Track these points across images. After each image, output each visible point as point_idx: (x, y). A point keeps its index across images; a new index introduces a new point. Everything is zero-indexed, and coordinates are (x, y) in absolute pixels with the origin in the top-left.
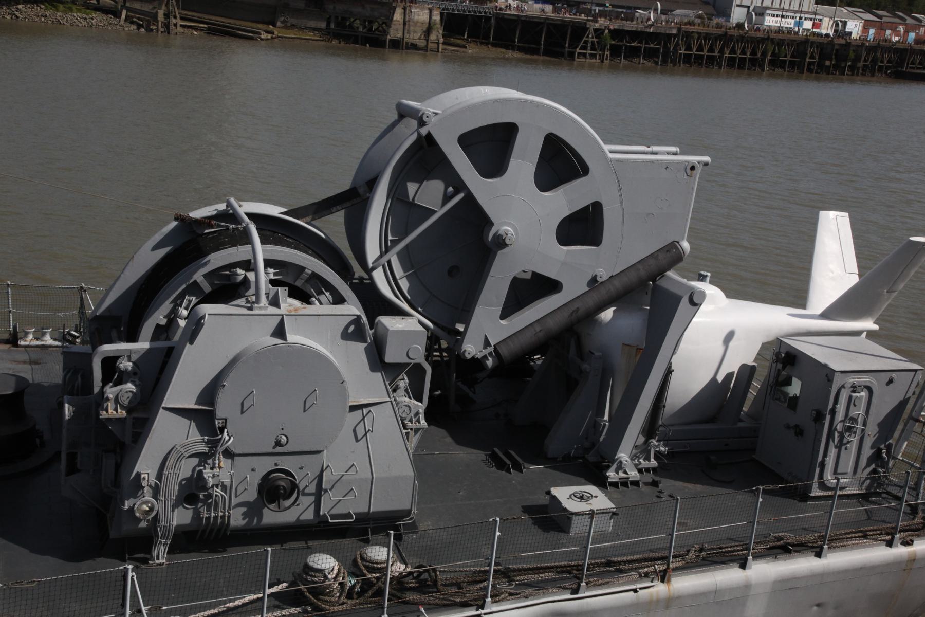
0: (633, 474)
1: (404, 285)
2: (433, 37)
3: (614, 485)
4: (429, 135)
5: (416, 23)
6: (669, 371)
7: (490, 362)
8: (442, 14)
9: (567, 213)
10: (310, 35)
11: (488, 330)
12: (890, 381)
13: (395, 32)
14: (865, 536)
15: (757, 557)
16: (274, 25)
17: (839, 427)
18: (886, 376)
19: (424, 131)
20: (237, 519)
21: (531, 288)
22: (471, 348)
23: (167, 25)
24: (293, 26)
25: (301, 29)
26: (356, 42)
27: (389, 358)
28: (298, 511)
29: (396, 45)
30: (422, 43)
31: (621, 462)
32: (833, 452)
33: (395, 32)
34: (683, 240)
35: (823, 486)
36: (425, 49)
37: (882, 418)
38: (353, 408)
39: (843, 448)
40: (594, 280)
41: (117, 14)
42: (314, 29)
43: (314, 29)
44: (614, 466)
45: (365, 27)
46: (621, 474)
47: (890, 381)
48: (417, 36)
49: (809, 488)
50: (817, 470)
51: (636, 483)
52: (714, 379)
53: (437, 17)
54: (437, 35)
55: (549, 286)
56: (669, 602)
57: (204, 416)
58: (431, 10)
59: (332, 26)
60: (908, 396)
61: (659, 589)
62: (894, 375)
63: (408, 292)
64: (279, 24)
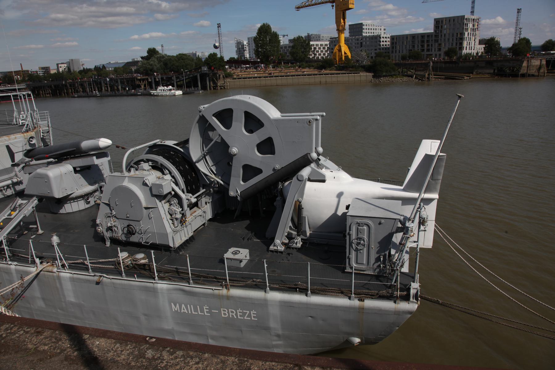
0: (281, 248)
1: (214, 169)
2: (542, 71)
3: (272, 251)
4: (203, 115)
5: (533, 66)
6: (299, 209)
7: (239, 198)
8: (547, 61)
9: (259, 142)
10: (487, 76)
11: (238, 187)
13: (523, 71)
14: (342, 293)
15: (272, 289)
16: (472, 73)
17: (355, 241)
18: (378, 220)
19: (201, 114)
20: (123, 238)
21: (250, 171)
22: (232, 193)
23: (428, 78)
24: (480, 73)
25: (483, 74)
26: (506, 76)
27: (154, 193)
28: (134, 239)
29: (523, 76)
30: (536, 74)
32: (353, 254)
33: (523, 71)
34: (312, 152)
36: (538, 76)
38: (146, 208)
40: (274, 170)
41: (412, 77)
42: (488, 73)
43: (488, 73)
44: (273, 244)
45: (510, 70)
46: (275, 248)
47: (380, 224)
48: (533, 71)
49: (345, 268)
50: (347, 260)
51: (281, 252)
52: (335, 215)
53: (544, 62)
54: (544, 70)
55: (259, 171)
56: (228, 298)
57: (108, 205)
58: (541, 60)
59: (496, 71)
61: (224, 291)
62: (383, 221)
63: (216, 171)
64: (474, 73)
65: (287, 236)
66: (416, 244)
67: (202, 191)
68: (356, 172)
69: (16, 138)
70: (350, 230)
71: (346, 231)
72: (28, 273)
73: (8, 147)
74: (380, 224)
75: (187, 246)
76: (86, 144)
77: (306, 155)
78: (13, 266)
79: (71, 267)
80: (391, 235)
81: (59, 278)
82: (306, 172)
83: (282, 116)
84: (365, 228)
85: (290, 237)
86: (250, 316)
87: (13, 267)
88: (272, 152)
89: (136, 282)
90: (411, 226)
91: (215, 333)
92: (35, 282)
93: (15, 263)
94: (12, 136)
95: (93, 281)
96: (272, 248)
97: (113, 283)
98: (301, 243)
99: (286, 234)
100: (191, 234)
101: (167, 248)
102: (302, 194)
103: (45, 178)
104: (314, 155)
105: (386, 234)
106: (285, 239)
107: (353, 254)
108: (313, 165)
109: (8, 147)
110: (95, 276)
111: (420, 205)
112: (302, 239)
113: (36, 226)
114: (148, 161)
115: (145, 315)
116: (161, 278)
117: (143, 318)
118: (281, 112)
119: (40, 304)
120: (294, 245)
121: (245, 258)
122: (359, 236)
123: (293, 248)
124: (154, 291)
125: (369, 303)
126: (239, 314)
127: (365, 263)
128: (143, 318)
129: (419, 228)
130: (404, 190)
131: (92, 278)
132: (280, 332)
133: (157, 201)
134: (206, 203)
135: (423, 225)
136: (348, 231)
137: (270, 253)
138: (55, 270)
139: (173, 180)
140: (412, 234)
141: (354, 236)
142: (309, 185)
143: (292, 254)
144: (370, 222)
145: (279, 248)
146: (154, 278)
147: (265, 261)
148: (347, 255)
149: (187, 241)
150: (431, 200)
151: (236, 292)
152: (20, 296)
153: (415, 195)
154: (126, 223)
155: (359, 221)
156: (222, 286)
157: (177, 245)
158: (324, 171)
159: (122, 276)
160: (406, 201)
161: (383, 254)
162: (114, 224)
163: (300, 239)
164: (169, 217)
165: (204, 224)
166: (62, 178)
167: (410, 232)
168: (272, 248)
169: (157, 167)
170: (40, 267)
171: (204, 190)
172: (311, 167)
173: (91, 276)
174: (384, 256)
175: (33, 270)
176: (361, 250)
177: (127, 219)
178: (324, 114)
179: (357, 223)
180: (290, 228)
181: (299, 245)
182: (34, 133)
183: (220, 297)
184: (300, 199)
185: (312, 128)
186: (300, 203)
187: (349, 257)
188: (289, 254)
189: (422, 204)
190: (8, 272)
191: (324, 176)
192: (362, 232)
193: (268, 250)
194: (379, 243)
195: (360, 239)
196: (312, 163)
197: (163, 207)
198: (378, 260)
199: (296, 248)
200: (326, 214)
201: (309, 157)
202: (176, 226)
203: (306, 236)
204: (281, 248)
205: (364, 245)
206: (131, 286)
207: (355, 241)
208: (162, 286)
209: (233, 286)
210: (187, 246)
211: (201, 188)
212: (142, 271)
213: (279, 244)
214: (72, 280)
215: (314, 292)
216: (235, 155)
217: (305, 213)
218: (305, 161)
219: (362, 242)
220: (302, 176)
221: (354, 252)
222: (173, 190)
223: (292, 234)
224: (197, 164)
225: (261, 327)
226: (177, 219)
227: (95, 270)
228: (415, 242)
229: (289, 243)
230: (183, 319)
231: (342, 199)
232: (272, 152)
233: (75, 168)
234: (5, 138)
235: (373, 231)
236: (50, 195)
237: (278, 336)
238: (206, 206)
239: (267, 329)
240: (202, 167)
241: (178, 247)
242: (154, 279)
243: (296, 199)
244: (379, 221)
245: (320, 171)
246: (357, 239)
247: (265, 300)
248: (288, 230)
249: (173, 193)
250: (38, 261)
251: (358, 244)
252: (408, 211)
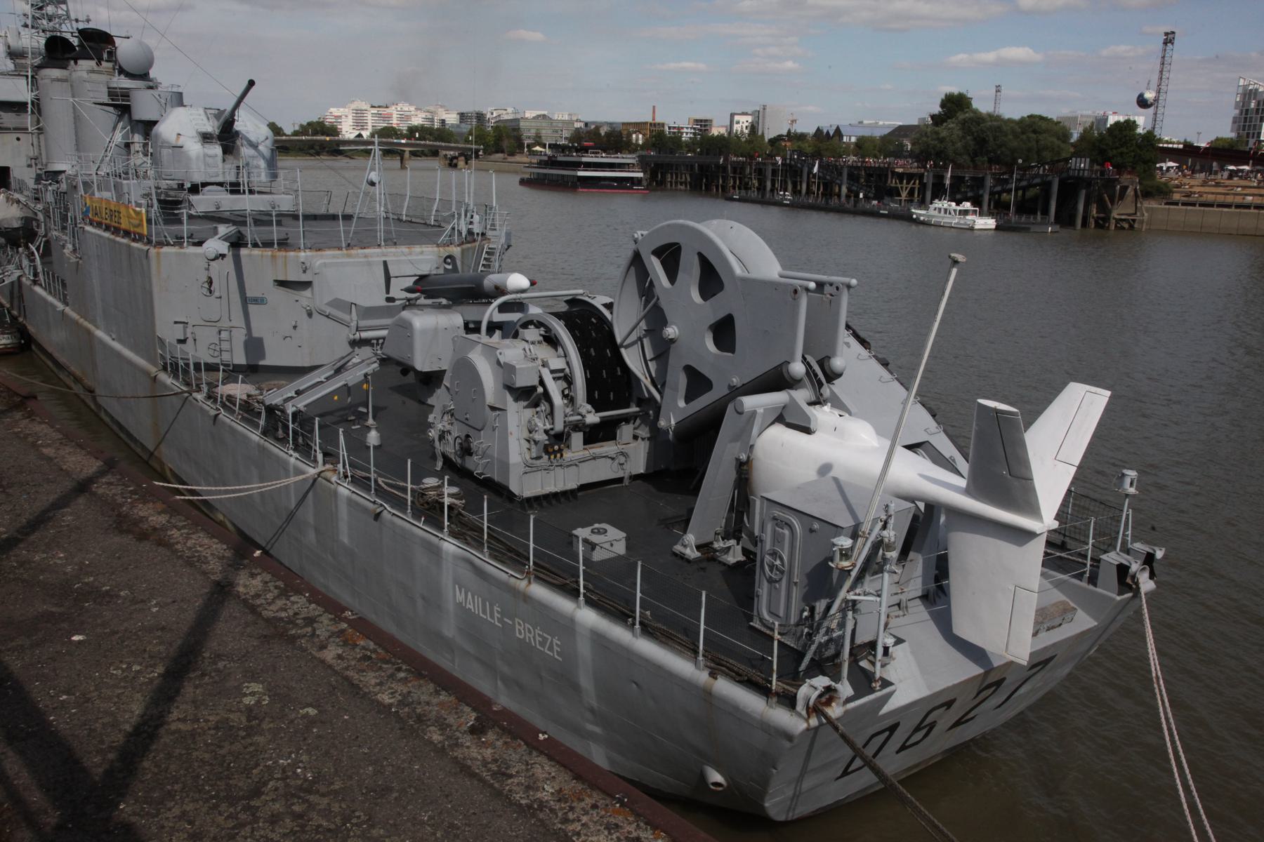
0: (692, 553)
3: (675, 554)
35: (761, 620)
38: (493, 408)
51: (688, 561)
56: (527, 598)
61: (522, 585)
67: (634, 409)
69: (422, 253)
72: (303, 473)
73: (385, 263)
75: (550, 504)
76: (491, 280)
78: (293, 458)
79: (355, 481)
81: (335, 493)
83: (781, 276)
86: (551, 648)
87: (292, 460)
88: (732, 349)
89: (420, 530)
91: (505, 669)
92: (310, 494)
93: (296, 455)
94: (417, 249)
95: (365, 510)
96: (678, 548)
97: (393, 523)
100: (572, 485)
101: (510, 496)
103: (407, 326)
109: (385, 263)
110: (374, 502)
113: (365, 410)
114: (539, 325)
115: (423, 598)
116: (453, 534)
117: (420, 603)
118: (784, 267)
119: (311, 536)
121: (607, 546)
124: (435, 552)
125: (726, 688)
126: (538, 638)
127: (781, 614)
128: (420, 603)
131: (371, 506)
132: (595, 704)
133: (509, 398)
134: (635, 437)
138: (334, 479)
139: (567, 370)
146: (441, 529)
147: (640, 563)
149: (555, 496)
151: (540, 591)
152: (291, 515)
154: (466, 430)
156: (522, 572)
157: (528, 493)
159: (405, 512)
162: (448, 427)
164: (526, 434)
165: (620, 480)
166: (433, 333)
169: (551, 340)
170: (321, 468)
171: (637, 409)
173: (367, 500)
175: (312, 471)
177: (465, 422)
178: (854, 282)
179: (775, 519)
182: (459, 249)
183: (514, 592)
190: (284, 465)
191: (808, 420)
197: (517, 416)
199: (724, 564)
202: (534, 455)
206: (413, 534)
208: (450, 546)
209: (538, 578)
210: (550, 504)
211: (633, 405)
212: (430, 510)
214: (350, 502)
215: (648, 631)
216: (672, 341)
221: (765, 584)
222: (542, 383)
224: (623, 350)
225: (565, 678)
226: (536, 443)
227: (380, 492)
230: (469, 622)
233: (466, 325)
234: (404, 249)
236: (410, 363)
237: (592, 711)
238: (634, 444)
239: (576, 687)
240: (632, 358)
241: (529, 500)
242: (441, 529)
247: (572, 620)
249: (540, 390)
250: (320, 457)
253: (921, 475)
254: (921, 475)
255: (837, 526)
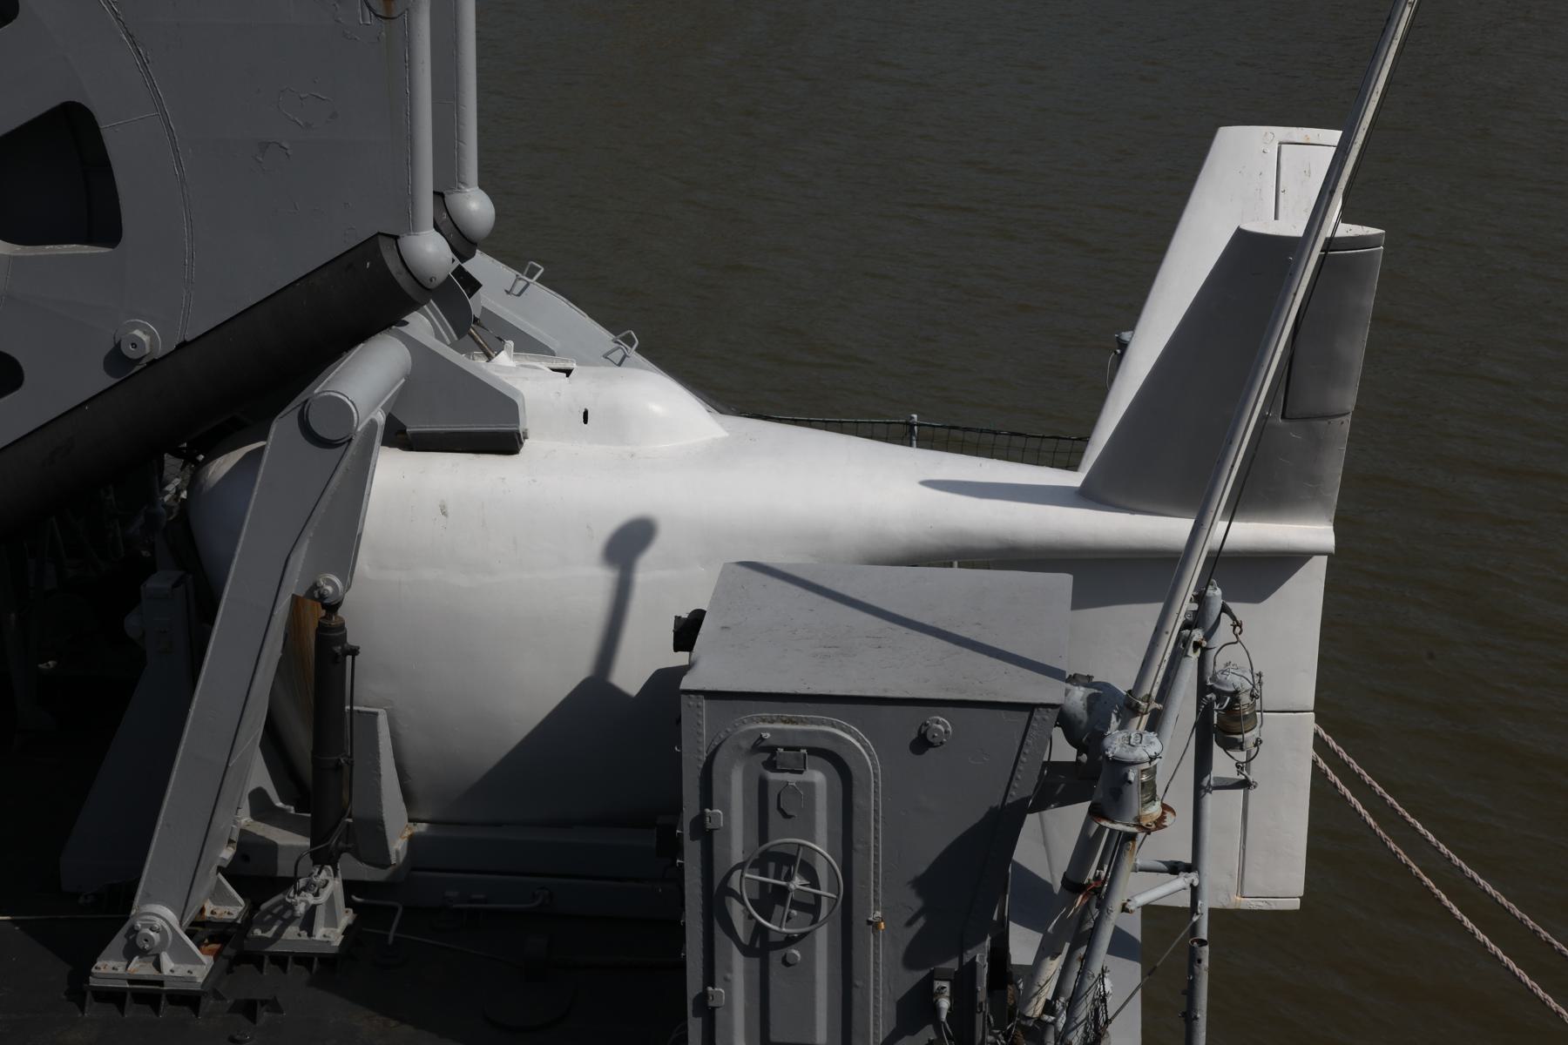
0: (189, 967)
6: (321, 654)
12: (922, 743)
17: (744, 882)
18: (910, 720)
31: (133, 931)
32: (738, 969)
34: (412, 226)
37: (923, 869)
39: (775, 957)
40: (116, 359)
44: (119, 941)
46: (140, 968)
51: (188, 999)
52: (596, 690)
60: (1015, 795)
65: (229, 872)
66: (1181, 882)
68: (751, 376)
70: (707, 799)
71: (678, 809)
74: (922, 743)
77: (370, 248)
80: (1002, 826)
82: (368, 378)
84: (817, 777)
85: (255, 874)
90: (1141, 753)
96: (110, 968)
98: (346, 918)
99: (227, 853)
102: (343, 537)
104: (430, 250)
105: (972, 815)
106: (218, 895)
107: (738, 969)
108: (422, 325)
111: (1201, 598)
112: (350, 887)
120: (292, 932)
122: (776, 841)
123: (280, 960)
129: (1203, 763)
130: (1087, 496)
135: (1230, 745)
136: (690, 809)
137: (93, 1010)
140: (1155, 810)
141: (737, 844)
142: (393, 471)
143: (274, 1006)
144: (849, 736)
145: (168, 964)
148: (694, 985)
150: (1286, 562)
153: (1170, 529)
155: (770, 727)
158: (503, 367)
160: (1103, 575)
161: (952, 965)
163: (335, 886)
167: (1135, 796)
168: (110, 968)
172: (410, 342)
174: (963, 983)
176: (790, 940)
179: (759, 746)
180: (261, 807)
181: (330, 934)
184: (331, 584)
185: (408, 41)
186: (332, 608)
187: (703, 997)
188: (249, 1009)
189: (1215, 593)
191: (508, 406)
192: (795, 808)
193: (79, 987)
194: (921, 885)
195: (785, 861)
196: (413, 305)
198: (915, 1009)
199: (304, 960)
200: (539, 684)
201: (393, 265)
203: (379, 856)
204: (189, 967)
205: (811, 908)
207: (744, 882)
213: (166, 934)
217: (370, 689)
218: (368, 294)
219: (797, 883)
220: (341, 409)
223: (272, 848)
228: (1174, 868)
229: (249, 921)
231: (647, 571)
232: (97, 220)
235: (870, 800)
243: (295, 584)
244: (913, 723)
245: (477, 365)
246: (760, 864)
248: (245, 819)
251: (770, 899)
252: (1116, 645)
253: (928, 484)
254: (928, 484)
255: (1030, 708)
